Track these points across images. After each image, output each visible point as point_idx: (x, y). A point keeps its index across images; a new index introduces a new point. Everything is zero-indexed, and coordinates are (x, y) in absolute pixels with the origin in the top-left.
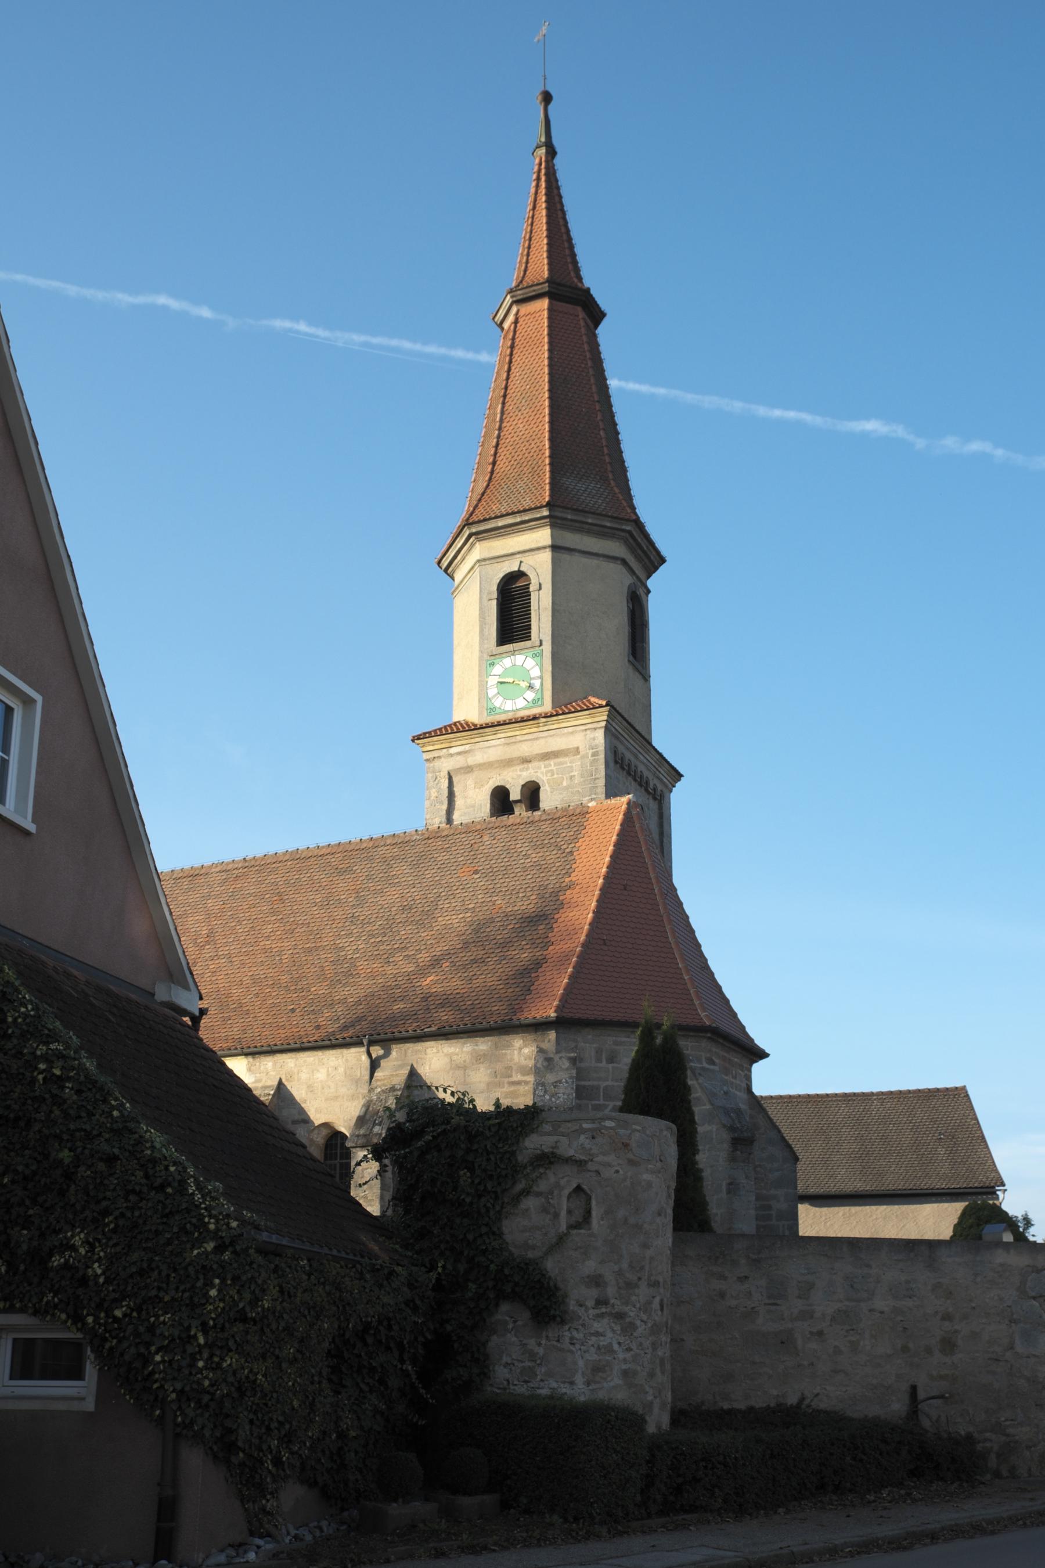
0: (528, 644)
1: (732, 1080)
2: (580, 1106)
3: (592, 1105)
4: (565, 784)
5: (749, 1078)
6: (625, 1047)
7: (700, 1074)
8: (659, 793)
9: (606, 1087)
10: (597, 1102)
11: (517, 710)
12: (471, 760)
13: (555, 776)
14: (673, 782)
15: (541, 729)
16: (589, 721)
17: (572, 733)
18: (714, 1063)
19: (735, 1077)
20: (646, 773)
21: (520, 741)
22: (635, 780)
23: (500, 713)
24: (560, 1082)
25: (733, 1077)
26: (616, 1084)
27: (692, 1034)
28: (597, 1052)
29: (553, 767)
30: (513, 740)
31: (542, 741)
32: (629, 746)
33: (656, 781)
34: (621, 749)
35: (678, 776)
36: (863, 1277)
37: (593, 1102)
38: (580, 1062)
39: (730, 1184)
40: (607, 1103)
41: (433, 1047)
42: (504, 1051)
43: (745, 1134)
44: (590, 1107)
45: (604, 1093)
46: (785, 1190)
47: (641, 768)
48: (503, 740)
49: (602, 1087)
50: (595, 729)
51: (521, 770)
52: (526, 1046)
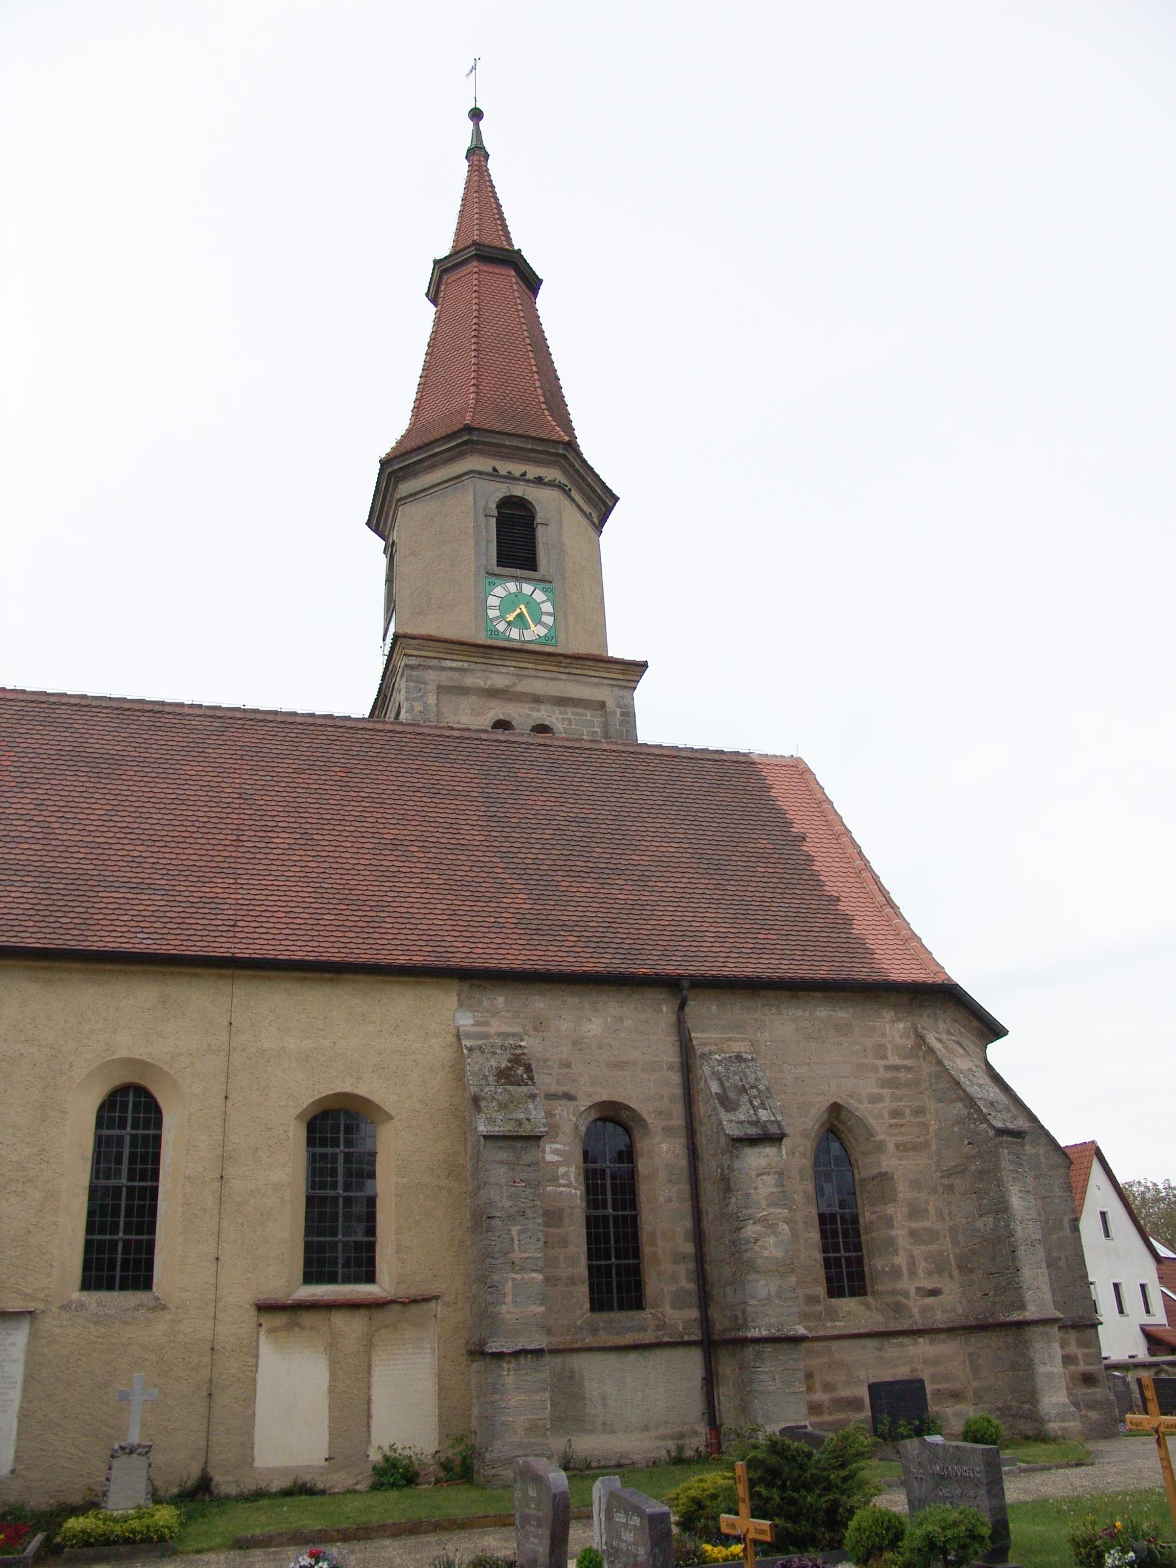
12: (469, 681)
15: (561, 670)
16: (620, 677)
17: (597, 684)
29: (569, 716)
30: (526, 672)
31: (561, 684)
41: (772, 1006)
42: (871, 1023)
48: (513, 669)
51: (532, 709)
52: (899, 1020)
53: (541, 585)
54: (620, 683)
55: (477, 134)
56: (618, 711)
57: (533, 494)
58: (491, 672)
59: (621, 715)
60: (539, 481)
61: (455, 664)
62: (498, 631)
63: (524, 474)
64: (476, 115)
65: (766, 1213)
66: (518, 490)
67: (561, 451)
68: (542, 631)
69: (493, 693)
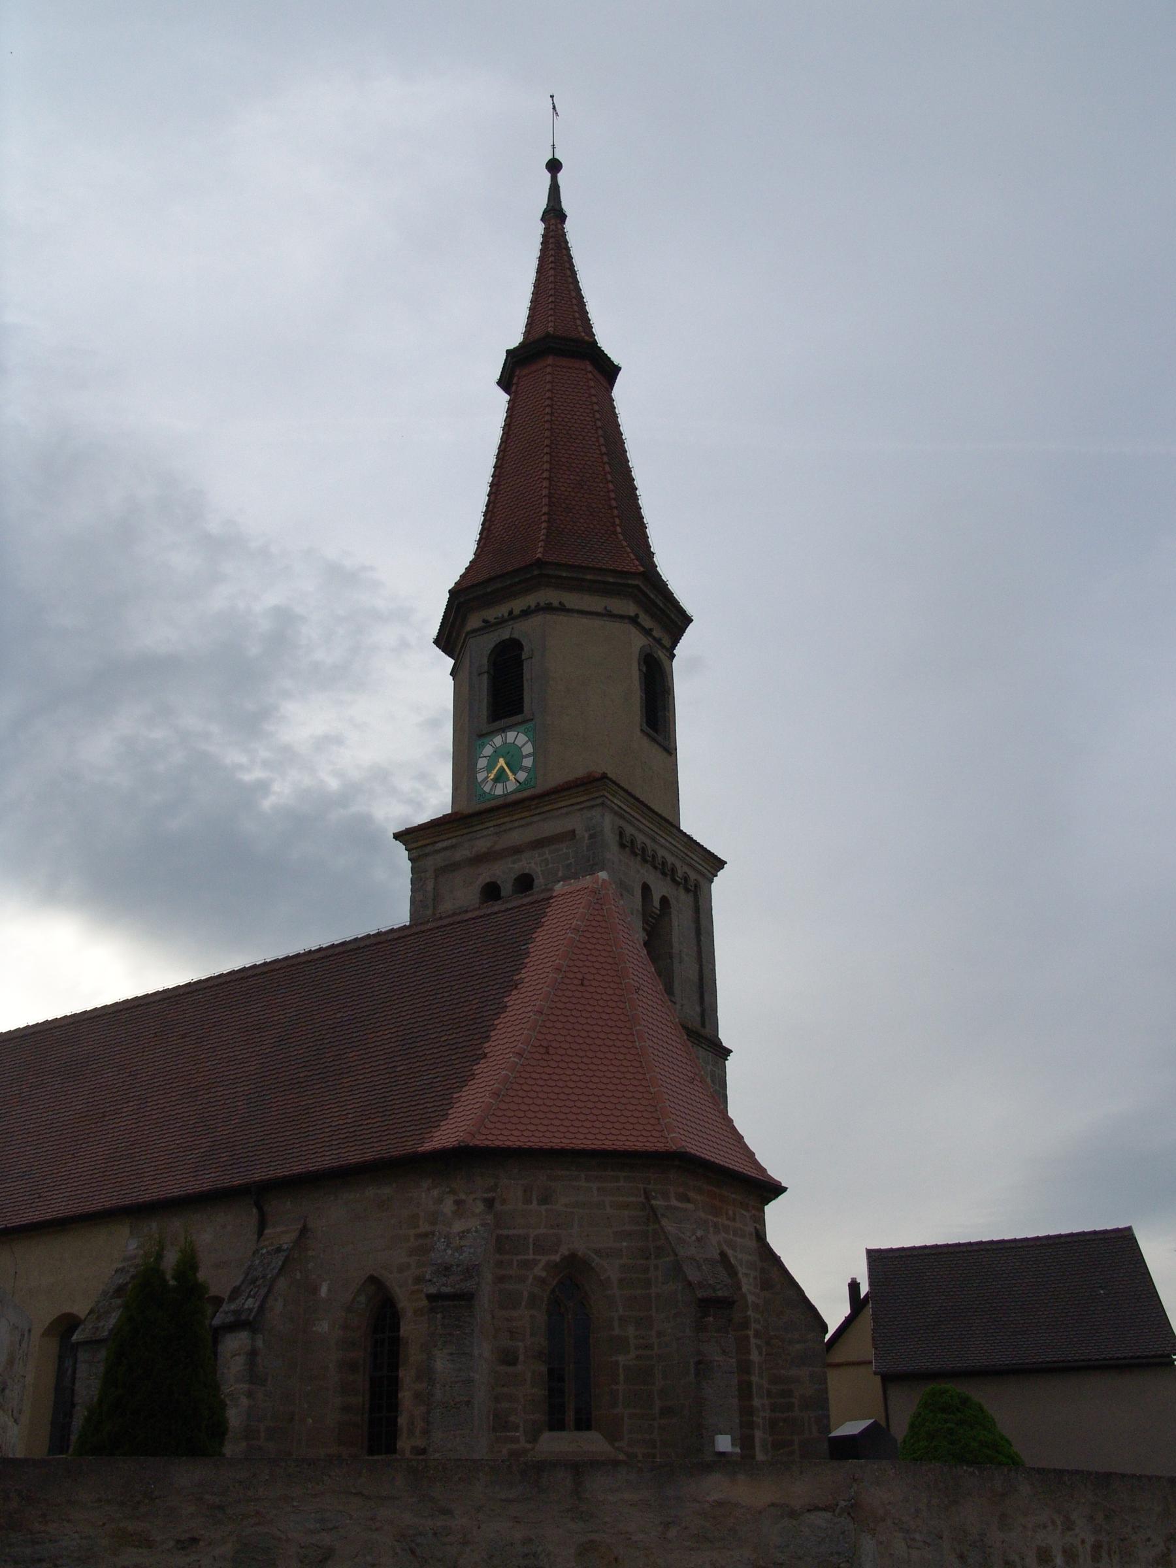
0: (519, 718)
1: (727, 1222)
2: (502, 1262)
3: (517, 1260)
4: (560, 874)
5: (761, 1220)
7: (663, 1215)
8: (692, 882)
10: (526, 1257)
11: (509, 794)
13: (550, 866)
14: (713, 871)
17: (567, 814)
18: (688, 1200)
19: (734, 1220)
20: (670, 859)
21: (510, 829)
22: (655, 868)
23: (489, 800)
24: (469, 1231)
25: (728, 1219)
28: (525, 1191)
30: (503, 828)
32: (642, 826)
33: (686, 869)
34: (629, 830)
35: (720, 864)
36: (435, 1534)
37: (519, 1257)
39: (698, 1363)
42: (410, 1195)
43: (720, 1294)
44: (515, 1263)
46: (810, 1369)
47: (661, 852)
50: (593, 807)
51: (514, 863)
53: (522, 728)
54: (588, 804)
55: (554, 190)
56: (587, 836)
57: (521, 630)
58: (477, 838)
59: (589, 839)
60: (526, 613)
61: (445, 844)
62: (485, 792)
63: (511, 613)
64: (554, 166)
65: (233, 1388)
66: (505, 634)
67: (536, 573)
68: (522, 776)
69: (480, 859)
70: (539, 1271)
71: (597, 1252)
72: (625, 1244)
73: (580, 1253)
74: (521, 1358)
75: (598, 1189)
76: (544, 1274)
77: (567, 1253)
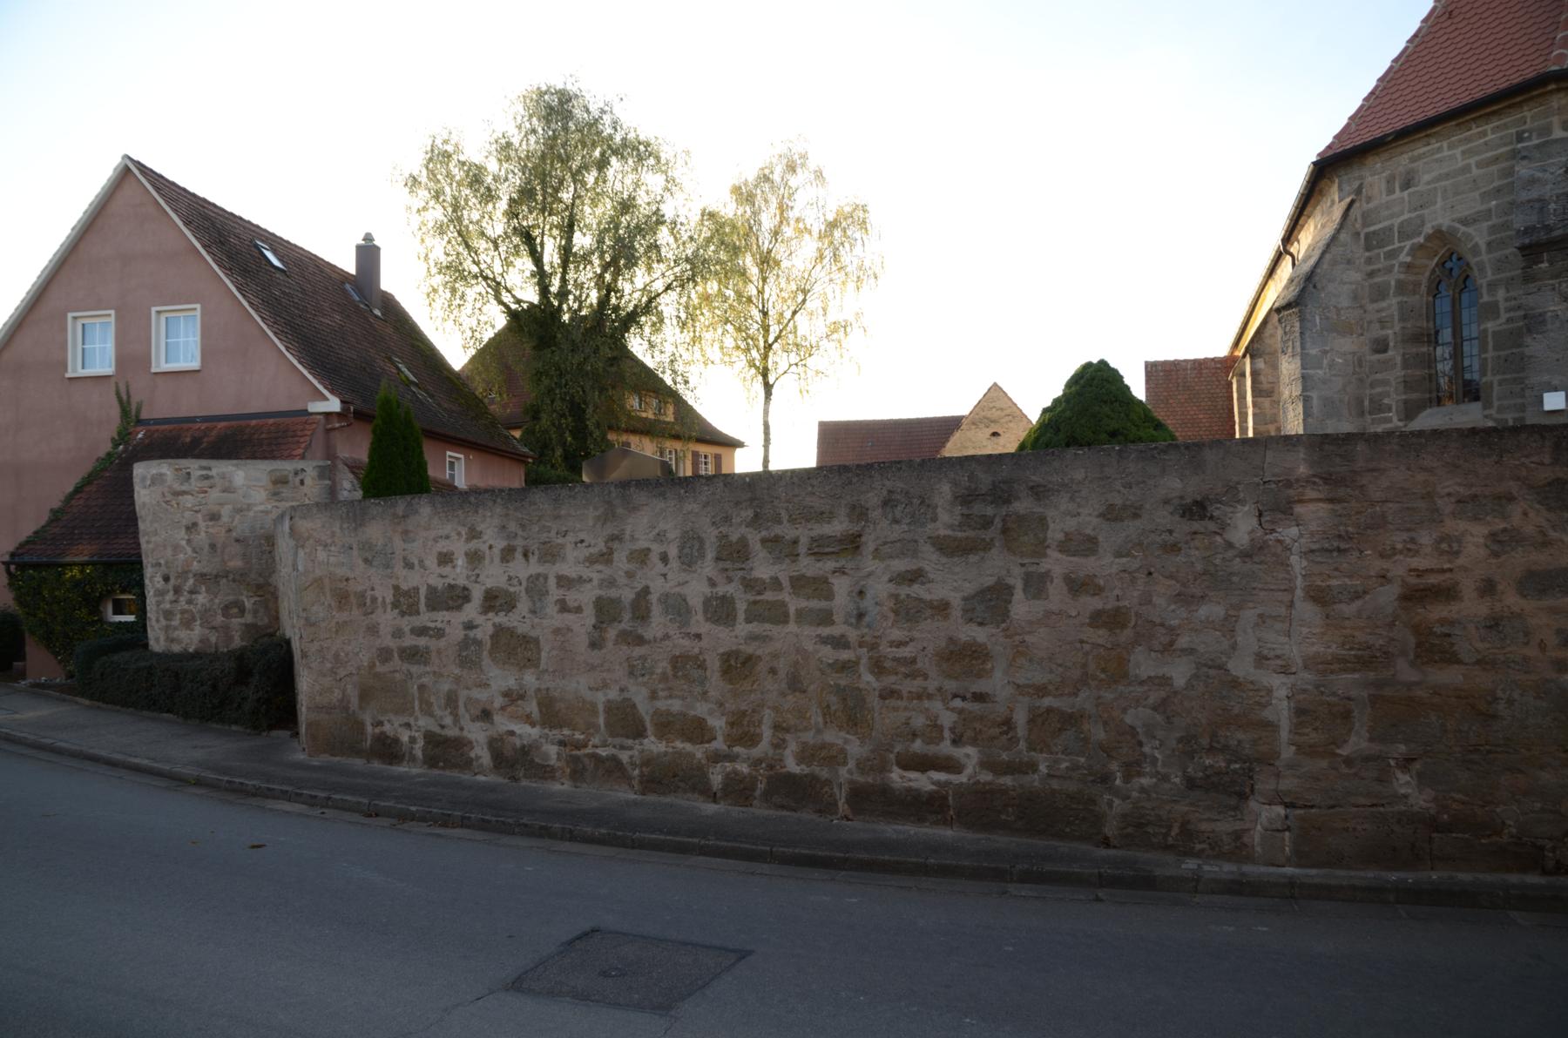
6: (1425, 160)
9: (1402, 223)
26: (1413, 215)
27: (1519, 99)
38: (1368, 203)
40: (1403, 244)
45: (1399, 232)
49: (1396, 225)
70: (1404, 258)
71: (1465, 222)
72: (1494, 203)
73: (1444, 229)
74: (1391, 344)
75: (1463, 153)
76: (1408, 259)
77: (1430, 231)
